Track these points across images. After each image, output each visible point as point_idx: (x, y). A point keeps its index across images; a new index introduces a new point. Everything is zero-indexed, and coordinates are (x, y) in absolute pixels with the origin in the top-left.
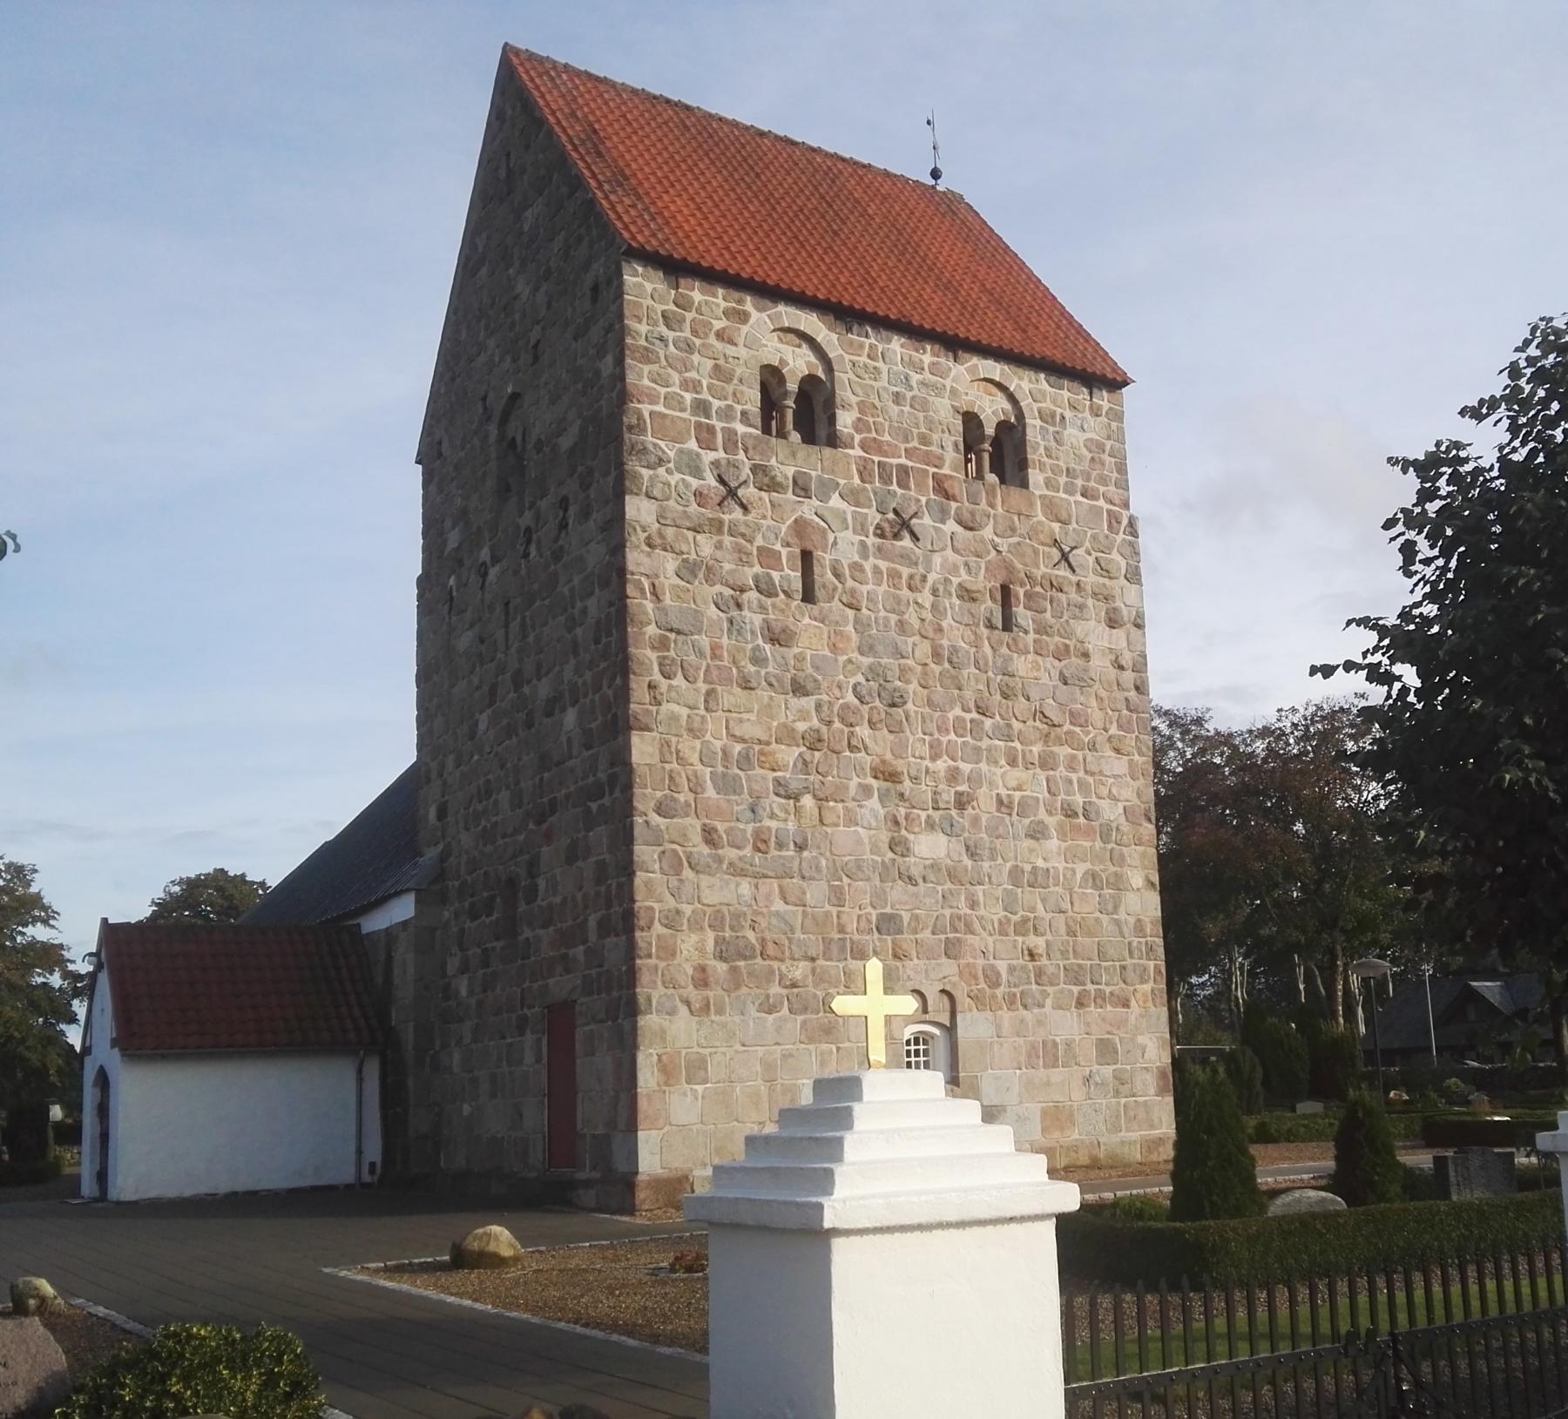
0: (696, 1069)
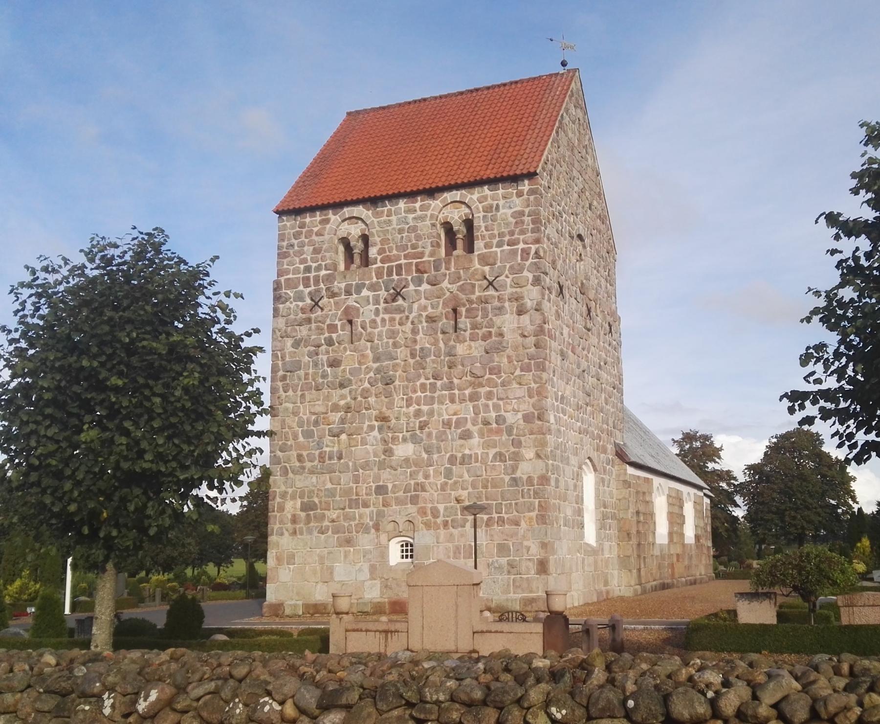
0: (291, 559)
